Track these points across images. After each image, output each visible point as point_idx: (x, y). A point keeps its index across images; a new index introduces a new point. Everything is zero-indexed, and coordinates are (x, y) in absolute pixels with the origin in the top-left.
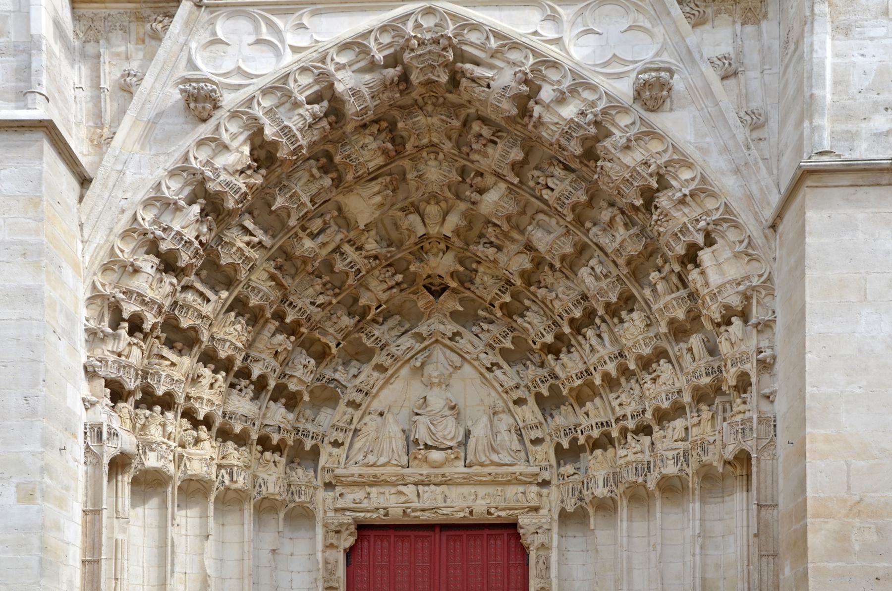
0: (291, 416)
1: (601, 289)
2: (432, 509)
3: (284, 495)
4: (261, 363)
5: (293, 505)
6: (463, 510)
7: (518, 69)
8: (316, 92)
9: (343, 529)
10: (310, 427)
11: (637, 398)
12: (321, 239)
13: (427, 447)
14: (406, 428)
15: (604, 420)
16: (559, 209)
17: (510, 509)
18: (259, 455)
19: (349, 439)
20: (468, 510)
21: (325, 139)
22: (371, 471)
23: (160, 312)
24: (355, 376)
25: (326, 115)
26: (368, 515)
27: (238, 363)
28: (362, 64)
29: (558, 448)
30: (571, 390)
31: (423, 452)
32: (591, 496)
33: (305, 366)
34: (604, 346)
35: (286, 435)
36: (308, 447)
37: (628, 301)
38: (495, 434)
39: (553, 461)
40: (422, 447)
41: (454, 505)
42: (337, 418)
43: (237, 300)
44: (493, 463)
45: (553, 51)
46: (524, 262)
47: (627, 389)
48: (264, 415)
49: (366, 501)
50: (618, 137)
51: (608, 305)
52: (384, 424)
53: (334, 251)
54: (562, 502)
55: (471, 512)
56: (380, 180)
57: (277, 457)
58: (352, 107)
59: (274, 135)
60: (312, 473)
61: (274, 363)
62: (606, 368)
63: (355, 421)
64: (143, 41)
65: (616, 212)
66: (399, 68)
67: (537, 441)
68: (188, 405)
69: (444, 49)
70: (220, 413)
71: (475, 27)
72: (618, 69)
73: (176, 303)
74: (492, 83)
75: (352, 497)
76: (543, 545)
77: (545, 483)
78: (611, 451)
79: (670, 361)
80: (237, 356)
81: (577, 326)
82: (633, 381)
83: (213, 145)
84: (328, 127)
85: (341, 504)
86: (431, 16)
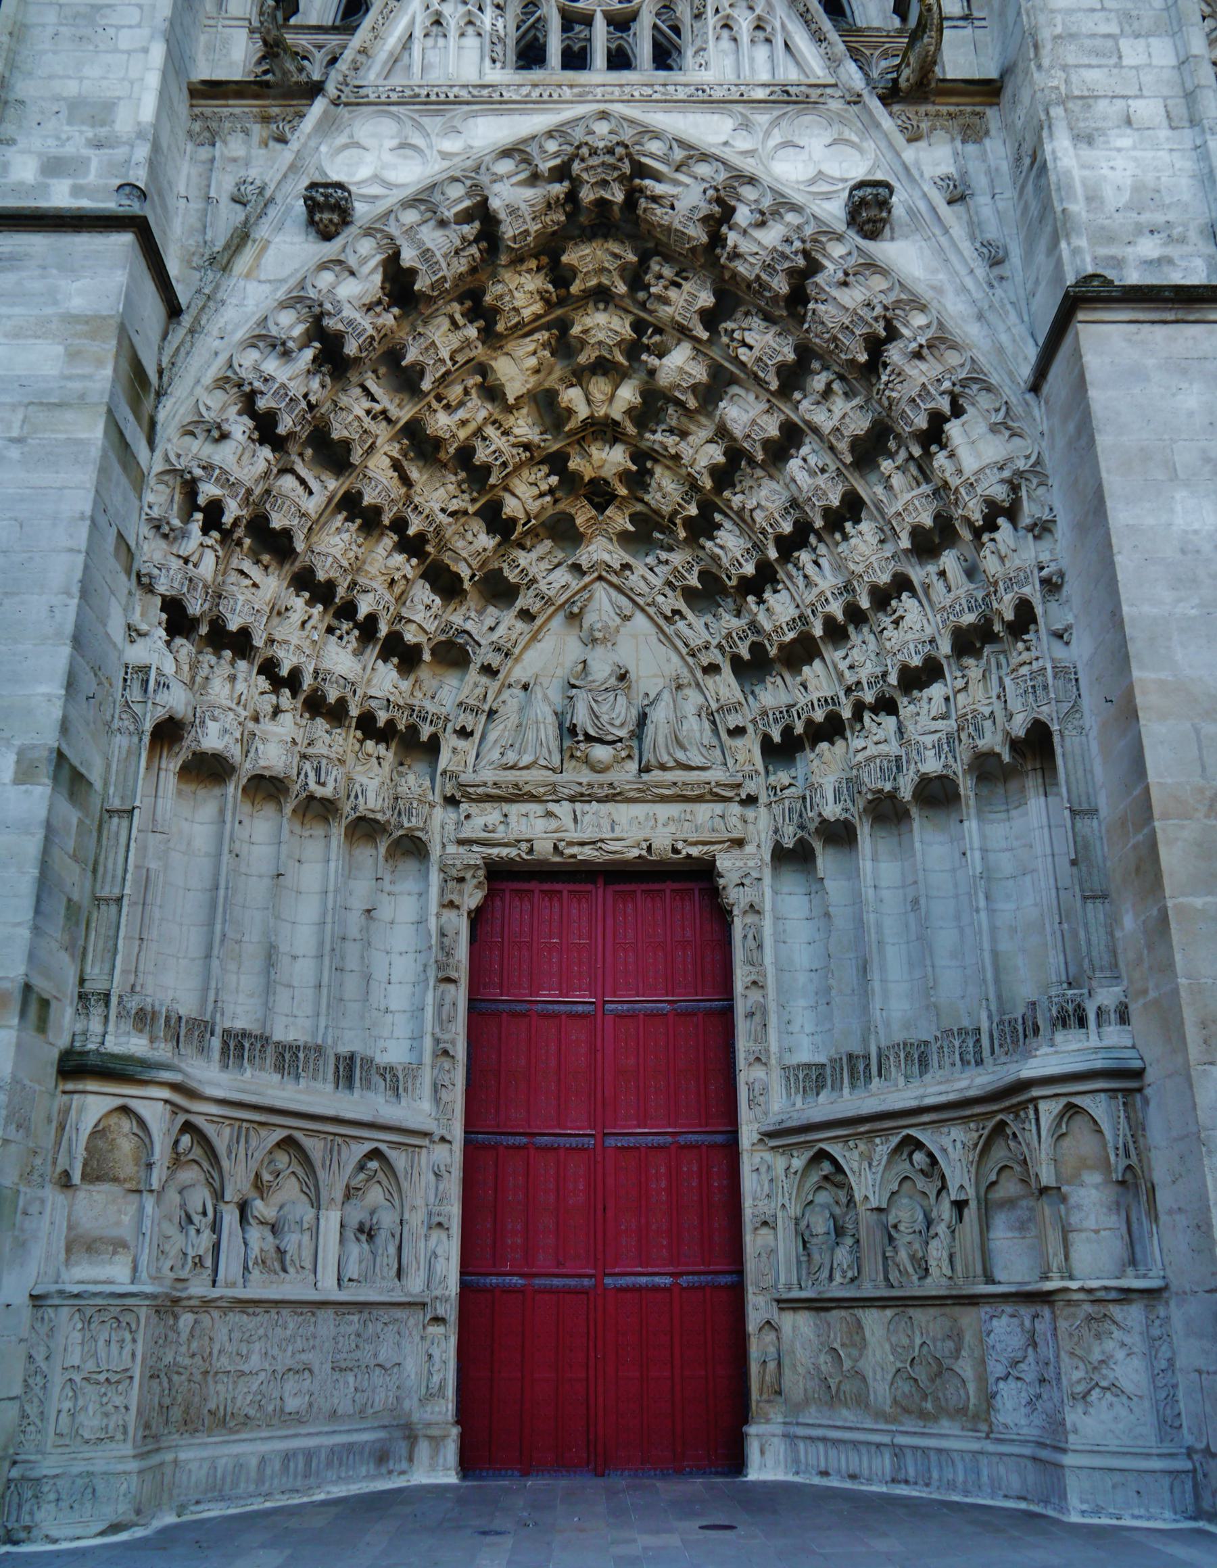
0: (405, 685)
1: (817, 488)
2: (594, 843)
3: (389, 813)
4: (371, 595)
5: (401, 832)
6: (638, 845)
7: (706, 185)
8: (467, 209)
9: (468, 876)
10: (431, 707)
11: (873, 656)
12: (461, 414)
13: (589, 738)
14: (559, 710)
15: (829, 694)
16: (761, 374)
17: (704, 843)
18: (357, 746)
19: (481, 727)
20: (645, 845)
21: (473, 270)
22: (511, 776)
23: (246, 501)
24: (492, 629)
25: (477, 240)
26: (504, 852)
27: (341, 591)
28: (522, 176)
29: (766, 741)
30: (782, 647)
31: (582, 746)
32: (818, 820)
33: (428, 607)
34: (824, 577)
35: (397, 714)
36: (424, 737)
37: (852, 507)
38: (681, 719)
39: (760, 768)
40: (581, 738)
41: (625, 835)
42: (466, 692)
43: (347, 494)
46: (715, 454)
47: (859, 642)
48: (369, 681)
49: (501, 828)
50: (831, 271)
52: (529, 701)
53: (474, 434)
54: (776, 831)
55: (649, 848)
56: (536, 336)
57: (382, 748)
59: (412, 259)
60: (428, 783)
62: (828, 609)
63: (490, 697)
64: (266, 145)
65: (832, 377)
67: (738, 732)
68: (269, 653)
69: (620, 160)
70: (311, 670)
71: (656, 135)
72: (825, 188)
73: (268, 492)
74: (676, 203)
75: (484, 818)
76: (752, 906)
77: (751, 800)
78: (840, 743)
79: (914, 594)
80: (340, 580)
81: (789, 545)
82: (866, 630)
83: (337, 268)
84: (478, 255)
85: (466, 833)
86: (604, 123)
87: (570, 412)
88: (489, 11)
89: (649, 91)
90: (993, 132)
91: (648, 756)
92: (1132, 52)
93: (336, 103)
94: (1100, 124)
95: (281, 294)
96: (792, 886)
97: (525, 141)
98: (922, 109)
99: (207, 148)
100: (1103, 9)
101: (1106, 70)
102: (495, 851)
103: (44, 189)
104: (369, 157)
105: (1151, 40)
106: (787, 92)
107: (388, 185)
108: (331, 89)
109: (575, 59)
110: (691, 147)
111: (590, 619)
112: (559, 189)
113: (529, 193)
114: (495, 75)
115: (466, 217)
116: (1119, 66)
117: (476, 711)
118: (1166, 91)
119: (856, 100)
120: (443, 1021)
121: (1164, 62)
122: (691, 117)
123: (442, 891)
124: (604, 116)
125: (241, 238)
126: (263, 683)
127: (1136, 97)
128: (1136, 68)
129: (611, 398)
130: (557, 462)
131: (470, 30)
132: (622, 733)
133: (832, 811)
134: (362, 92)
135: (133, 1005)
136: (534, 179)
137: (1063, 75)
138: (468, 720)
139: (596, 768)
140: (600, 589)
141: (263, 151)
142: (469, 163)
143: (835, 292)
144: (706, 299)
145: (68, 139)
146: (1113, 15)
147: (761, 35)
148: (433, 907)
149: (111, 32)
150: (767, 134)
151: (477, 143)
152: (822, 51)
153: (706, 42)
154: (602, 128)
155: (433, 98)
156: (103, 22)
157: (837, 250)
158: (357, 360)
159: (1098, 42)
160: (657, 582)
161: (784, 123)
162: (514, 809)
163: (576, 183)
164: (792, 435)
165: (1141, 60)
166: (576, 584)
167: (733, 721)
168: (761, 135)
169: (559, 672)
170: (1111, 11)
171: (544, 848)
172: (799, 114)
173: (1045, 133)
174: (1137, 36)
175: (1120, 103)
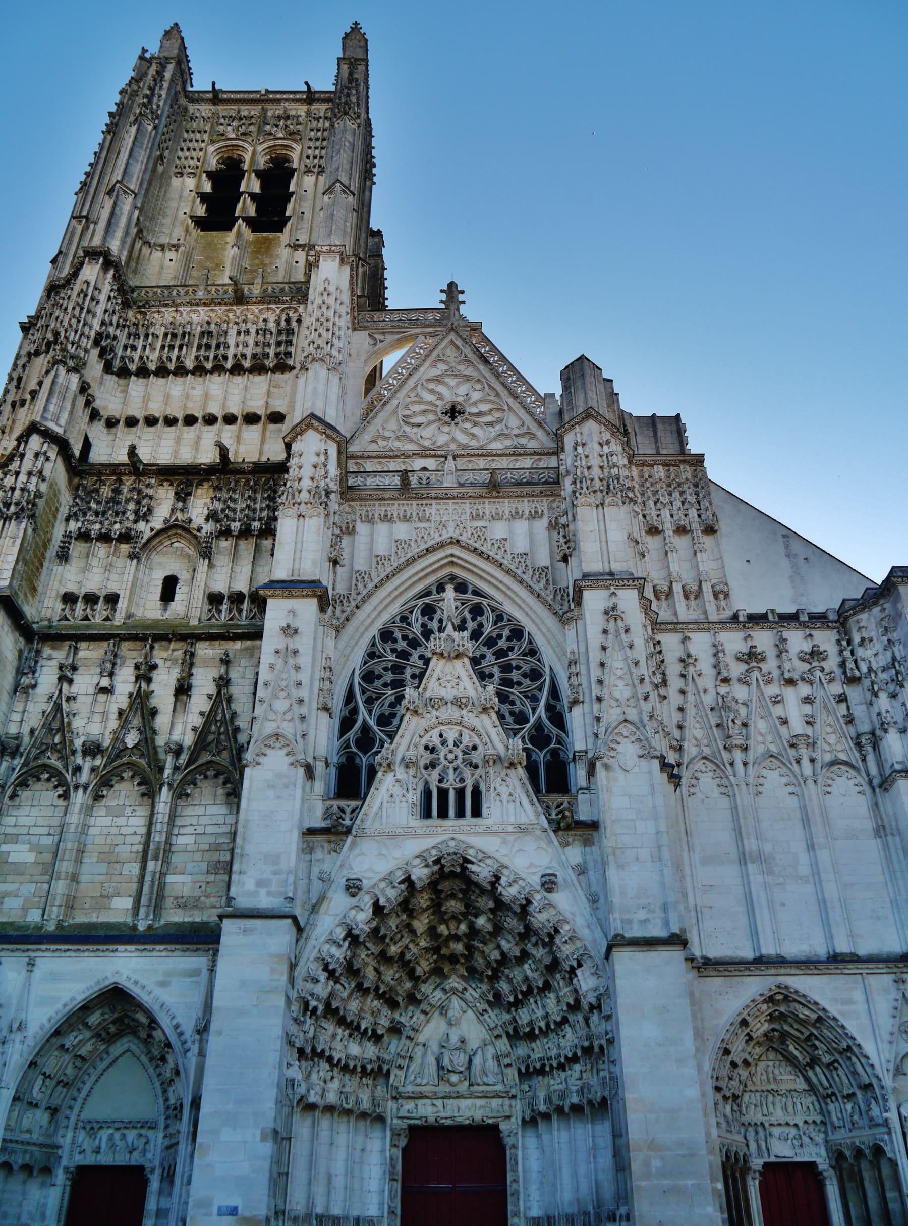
26: (416, 1122)
44: (485, 1084)
45: (505, 861)
51: (538, 987)
58: (418, 885)
61: (372, 1019)
87: (441, 935)
88: (411, 791)
91: (473, 1080)
95: (337, 922)
96: (530, 1134)
102: (412, 1122)
103: (255, 894)
107: (375, 872)
108: (354, 832)
109: (443, 814)
111: (450, 1013)
113: (426, 871)
115: (400, 883)
117: (404, 1058)
119: (546, 830)
120: (392, 1198)
123: (391, 1140)
124: (453, 839)
125: (322, 899)
126: (327, 1067)
129: (458, 928)
130: (436, 950)
132: (462, 1069)
133: (542, 1108)
135: (292, 1215)
138: (400, 1062)
139: (452, 1085)
140: (455, 1000)
143: (536, 915)
144: (491, 904)
148: (388, 1147)
154: (452, 844)
157: (538, 897)
158: (364, 942)
160: (476, 996)
162: (420, 1102)
163: (443, 866)
164: (525, 956)
166: (444, 997)
167: (507, 1061)
169: (438, 1037)
171: (432, 1120)
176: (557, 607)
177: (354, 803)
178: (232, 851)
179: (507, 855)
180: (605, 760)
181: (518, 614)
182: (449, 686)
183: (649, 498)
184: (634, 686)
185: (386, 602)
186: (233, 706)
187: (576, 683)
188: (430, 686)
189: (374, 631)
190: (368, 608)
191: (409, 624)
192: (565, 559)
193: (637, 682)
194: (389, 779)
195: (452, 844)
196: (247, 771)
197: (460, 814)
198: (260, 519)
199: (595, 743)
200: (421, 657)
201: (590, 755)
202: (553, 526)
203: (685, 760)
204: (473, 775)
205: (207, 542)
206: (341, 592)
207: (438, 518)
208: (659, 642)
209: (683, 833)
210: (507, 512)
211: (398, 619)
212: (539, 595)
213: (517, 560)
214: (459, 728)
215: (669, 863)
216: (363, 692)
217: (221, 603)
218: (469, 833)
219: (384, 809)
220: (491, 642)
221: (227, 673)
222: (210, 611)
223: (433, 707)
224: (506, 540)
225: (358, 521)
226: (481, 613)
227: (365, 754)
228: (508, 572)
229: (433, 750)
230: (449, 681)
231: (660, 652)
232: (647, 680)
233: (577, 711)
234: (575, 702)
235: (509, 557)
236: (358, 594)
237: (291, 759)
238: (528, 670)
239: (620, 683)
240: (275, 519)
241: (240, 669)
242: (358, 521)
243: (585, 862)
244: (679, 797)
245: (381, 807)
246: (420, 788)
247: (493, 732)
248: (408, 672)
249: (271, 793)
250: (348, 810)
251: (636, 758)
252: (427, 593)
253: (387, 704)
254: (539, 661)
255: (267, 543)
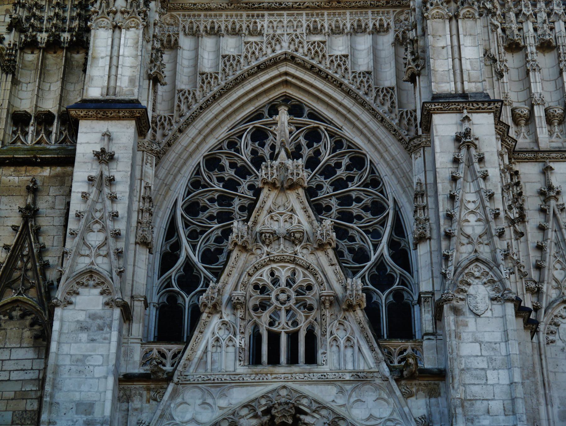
28: (251, 415)
64: (149, 402)
66: (269, 416)
69: (291, 408)
71: (306, 397)
89: (302, 376)
90: (442, 394)
92: (492, 376)
93: (177, 384)
94: (477, 413)
97: (253, 401)
98: (414, 382)
99: (126, 404)
100: (481, 356)
101: (481, 386)
104: (190, 409)
105: (500, 371)
106: (358, 376)
108: (175, 379)
109: (274, 360)
110: (319, 403)
112: (266, 419)
114: (241, 370)
116: (486, 384)
118: (504, 397)
119: (387, 379)
121: (504, 383)
122: (320, 387)
124: (284, 387)
127: (492, 400)
128: (493, 385)
131: (231, 344)
134: (188, 378)
136: (256, 416)
137: (464, 389)
141: (147, 405)
142: (230, 412)
145: (77, 421)
146: (485, 359)
147: (349, 344)
149: (91, 368)
150: (350, 396)
151: (233, 402)
152: (373, 354)
153: (326, 350)
154: (284, 393)
155: (216, 381)
156: (88, 364)
159: (478, 372)
161: (357, 390)
163: (273, 417)
165: (495, 381)
168: (347, 397)
170: (484, 356)
172: (364, 385)
173: (454, 420)
174: (494, 369)
175: (485, 402)
176: (403, 133)
177: (175, 347)
178: (40, 399)
179: (344, 406)
180: (454, 303)
181: (359, 141)
182: (282, 219)
183: (509, 9)
184: (488, 221)
185: (212, 126)
186: (41, 239)
187: (423, 217)
188: (261, 219)
189: (199, 158)
190: (192, 132)
191: (238, 151)
192: (412, 79)
193: (490, 217)
194: (215, 321)
195: (284, 393)
196: (58, 312)
197: (293, 360)
198: (71, 30)
199: (443, 284)
200: (251, 187)
201: (437, 297)
202: (399, 42)
203: (544, 305)
204: (307, 317)
205: (10, 55)
206: (162, 113)
207: (271, 32)
208: (517, 173)
209: (540, 384)
210: (348, 25)
211: (225, 145)
212: (383, 119)
213: (359, 80)
214: (292, 266)
215: (524, 417)
216: (187, 225)
217: (27, 125)
218: (303, 382)
219: (209, 355)
220: (328, 171)
221: (34, 201)
222: (14, 133)
223: (263, 242)
224: (346, 56)
225: (181, 34)
226: (319, 140)
227: (188, 293)
228: (348, 93)
229: (263, 289)
230: (281, 214)
231: (518, 184)
232: (502, 214)
233: (423, 249)
234: (421, 239)
235: (351, 76)
236: (181, 116)
237: (106, 299)
238: (369, 202)
239: (472, 218)
240: (88, 30)
241: (50, 199)
242: (181, 34)
243: (430, 414)
244: (536, 345)
245: (205, 352)
246: (249, 330)
247: (329, 271)
248: (237, 203)
249: (84, 336)
250: (169, 355)
251: (488, 301)
252: (258, 115)
253: (213, 238)
254: (382, 192)
255: (78, 57)
